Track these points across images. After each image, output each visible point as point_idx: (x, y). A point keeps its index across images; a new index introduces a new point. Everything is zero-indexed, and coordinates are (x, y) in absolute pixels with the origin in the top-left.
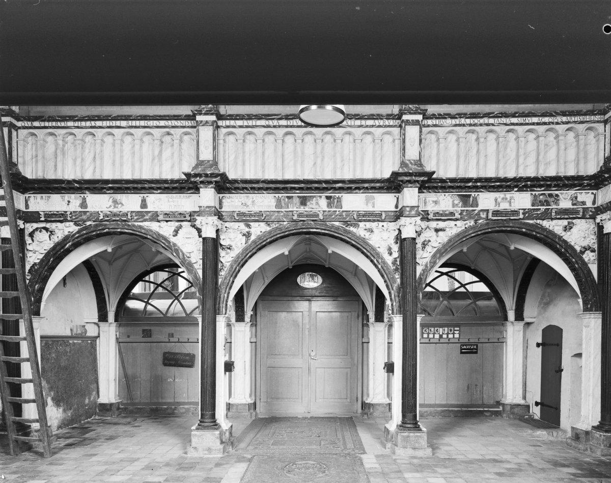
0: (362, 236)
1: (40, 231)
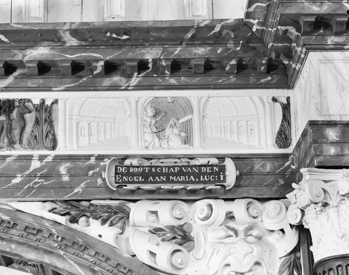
0: (144, 258)
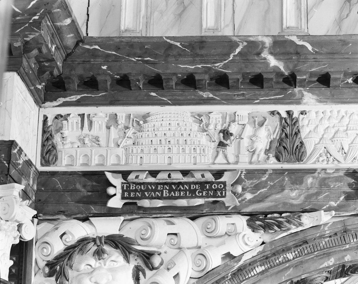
1: (99, 254)
